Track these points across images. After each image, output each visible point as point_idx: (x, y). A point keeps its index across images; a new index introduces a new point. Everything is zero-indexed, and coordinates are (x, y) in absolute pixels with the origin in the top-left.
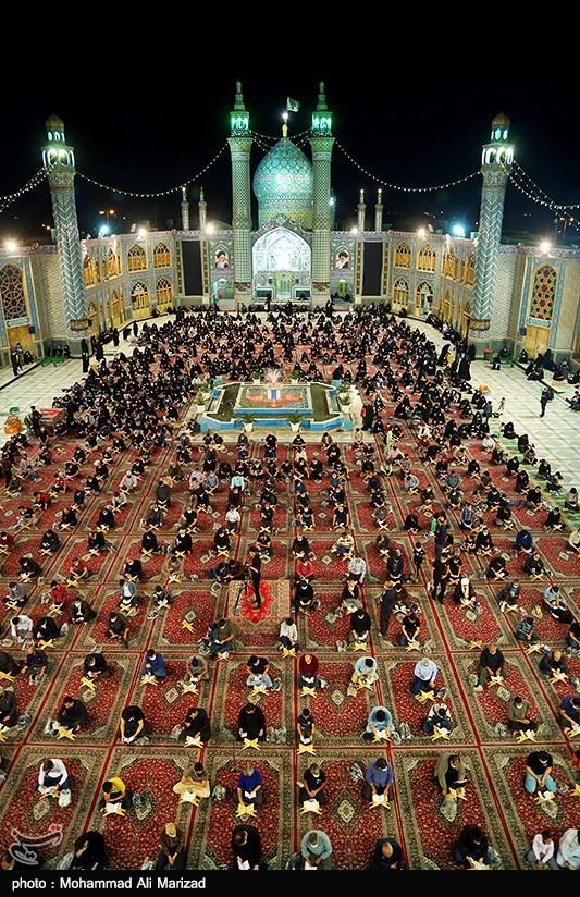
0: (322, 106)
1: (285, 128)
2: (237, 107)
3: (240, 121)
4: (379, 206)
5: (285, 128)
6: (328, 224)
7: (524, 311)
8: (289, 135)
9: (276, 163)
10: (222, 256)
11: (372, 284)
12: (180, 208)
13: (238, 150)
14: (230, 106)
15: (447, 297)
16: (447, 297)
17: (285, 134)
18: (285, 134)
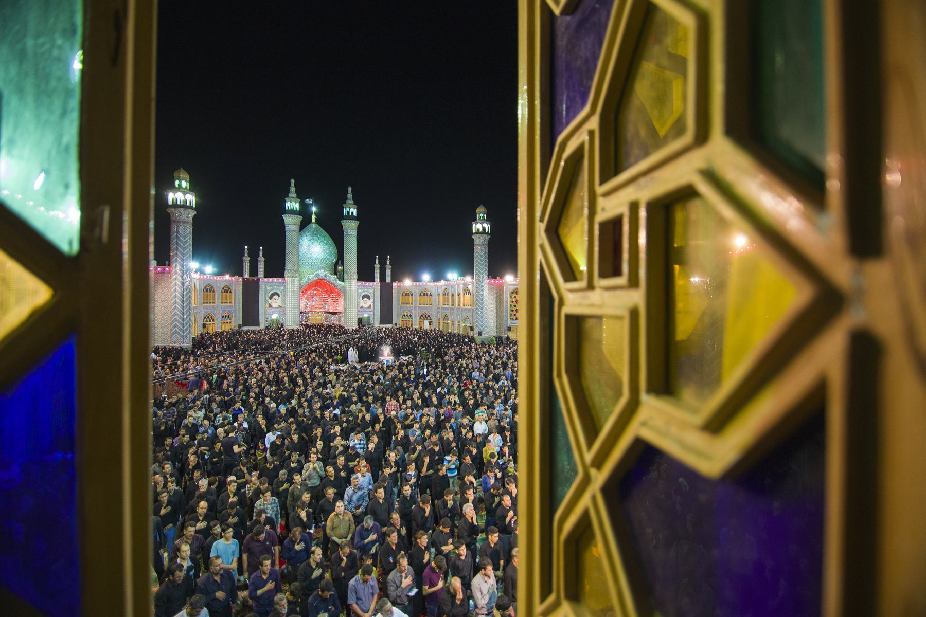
0: (352, 202)
1: (314, 217)
2: (290, 195)
3: (293, 204)
4: (388, 267)
5: (314, 217)
6: (356, 277)
7: (506, 316)
8: (317, 221)
9: (309, 237)
10: (276, 297)
11: (386, 316)
12: (242, 262)
13: (291, 222)
14: (286, 194)
15: (445, 317)
16: (445, 317)
17: (314, 220)
18: (314, 220)
